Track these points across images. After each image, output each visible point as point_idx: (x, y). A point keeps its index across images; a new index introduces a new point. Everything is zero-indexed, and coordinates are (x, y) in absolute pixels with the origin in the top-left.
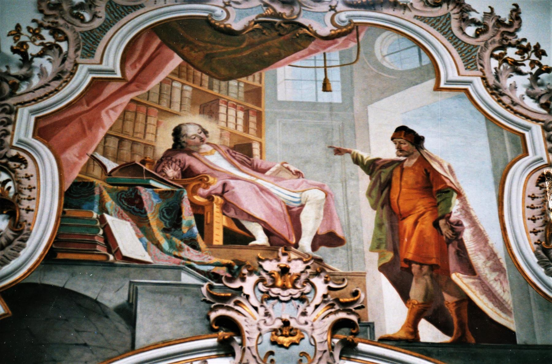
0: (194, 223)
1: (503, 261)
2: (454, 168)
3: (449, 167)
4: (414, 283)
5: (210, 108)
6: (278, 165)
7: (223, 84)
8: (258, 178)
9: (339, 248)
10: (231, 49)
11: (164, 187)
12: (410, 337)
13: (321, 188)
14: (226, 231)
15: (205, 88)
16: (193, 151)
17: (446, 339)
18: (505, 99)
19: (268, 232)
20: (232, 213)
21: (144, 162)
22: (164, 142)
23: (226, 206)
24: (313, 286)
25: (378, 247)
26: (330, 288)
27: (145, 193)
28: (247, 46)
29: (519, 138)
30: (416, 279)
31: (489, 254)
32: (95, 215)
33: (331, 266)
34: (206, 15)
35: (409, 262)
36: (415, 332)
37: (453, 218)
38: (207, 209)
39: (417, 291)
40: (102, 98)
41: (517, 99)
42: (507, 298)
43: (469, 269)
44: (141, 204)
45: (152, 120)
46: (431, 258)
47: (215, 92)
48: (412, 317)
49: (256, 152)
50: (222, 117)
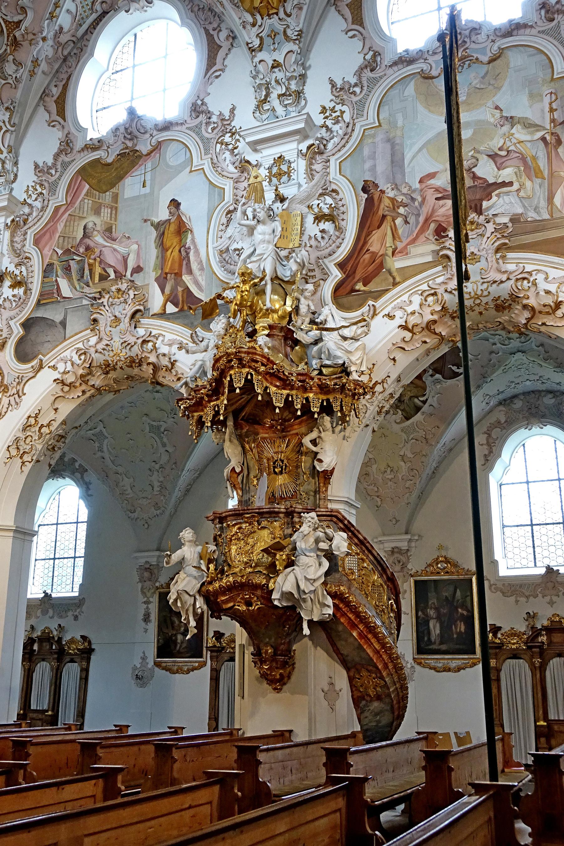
1: (204, 264)
5: (97, 212)
11: (78, 258)
17: (177, 310)
18: (219, 169)
19: (115, 272)
20: (103, 266)
21: (72, 248)
22: (80, 234)
23: (100, 263)
27: (72, 263)
32: (54, 279)
35: (166, 274)
36: (165, 310)
40: (58, 217)
41: (224, 166)
42: (203, 283)
43: (190, 272)
44: (70, 270)
45: (76, 224)
49: (114, 230)
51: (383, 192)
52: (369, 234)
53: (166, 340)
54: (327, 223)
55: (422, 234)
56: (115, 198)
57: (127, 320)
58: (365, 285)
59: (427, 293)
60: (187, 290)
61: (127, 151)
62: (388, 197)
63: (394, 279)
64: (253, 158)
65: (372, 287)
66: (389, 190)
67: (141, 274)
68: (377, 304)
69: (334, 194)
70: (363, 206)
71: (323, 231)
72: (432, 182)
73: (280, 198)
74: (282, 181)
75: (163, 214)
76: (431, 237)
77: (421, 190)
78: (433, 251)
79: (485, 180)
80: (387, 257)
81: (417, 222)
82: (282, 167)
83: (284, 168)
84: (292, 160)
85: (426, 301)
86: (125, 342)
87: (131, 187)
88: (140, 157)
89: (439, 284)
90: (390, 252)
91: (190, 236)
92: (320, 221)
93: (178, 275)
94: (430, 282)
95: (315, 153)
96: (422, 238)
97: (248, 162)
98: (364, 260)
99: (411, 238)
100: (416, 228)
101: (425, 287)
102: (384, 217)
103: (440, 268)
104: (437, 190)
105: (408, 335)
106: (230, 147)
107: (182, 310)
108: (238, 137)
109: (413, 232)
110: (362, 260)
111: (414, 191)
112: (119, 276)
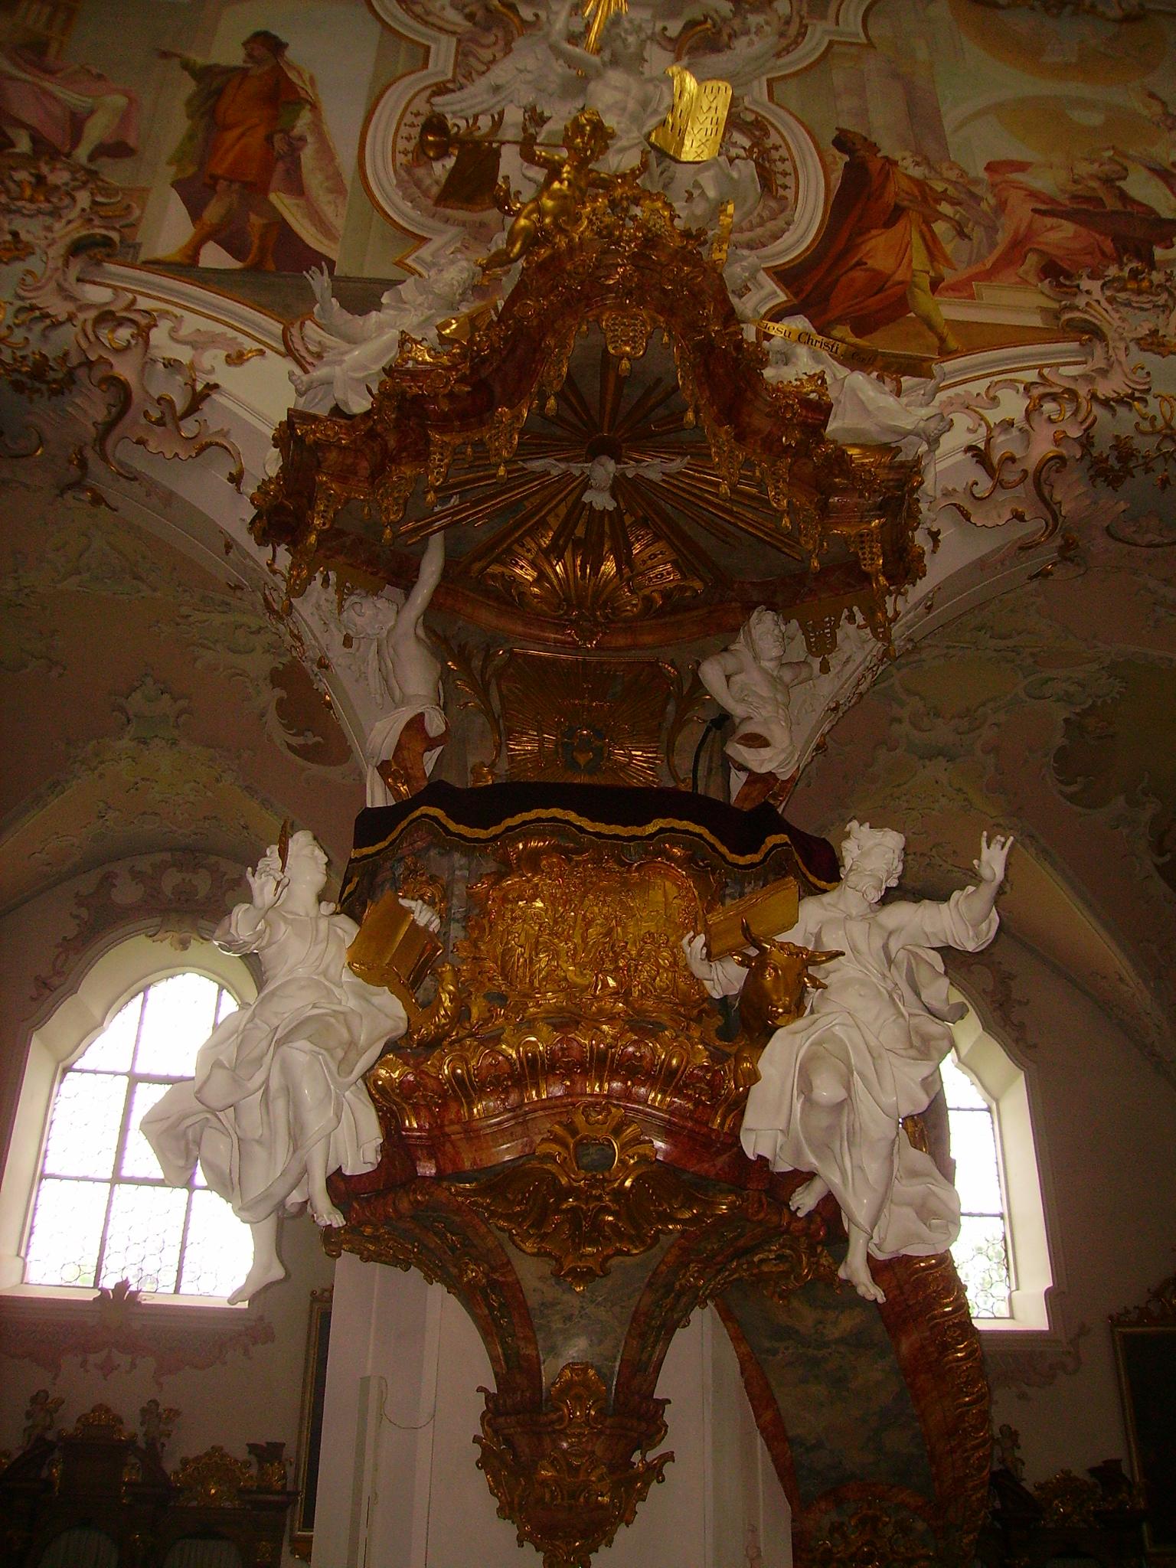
13: (126, 93)
35: (215, 179)
37: (296, 132)
39: (213, 213)
52: (862, 230)
53: (185, 331)
59: (1041, 390)
63: (942, 340)
66: (908, 162)
77: (994, 185)
78: (1043, 310)
79: (1152, 211)
81: (992, 246)
86: (33, 308)
90: (925, 281)
93: (256, 189)
100: (990, 253)
101: (1032, 376)
104: (1033, 194)
105: (985, 484)
111: (976, 182)
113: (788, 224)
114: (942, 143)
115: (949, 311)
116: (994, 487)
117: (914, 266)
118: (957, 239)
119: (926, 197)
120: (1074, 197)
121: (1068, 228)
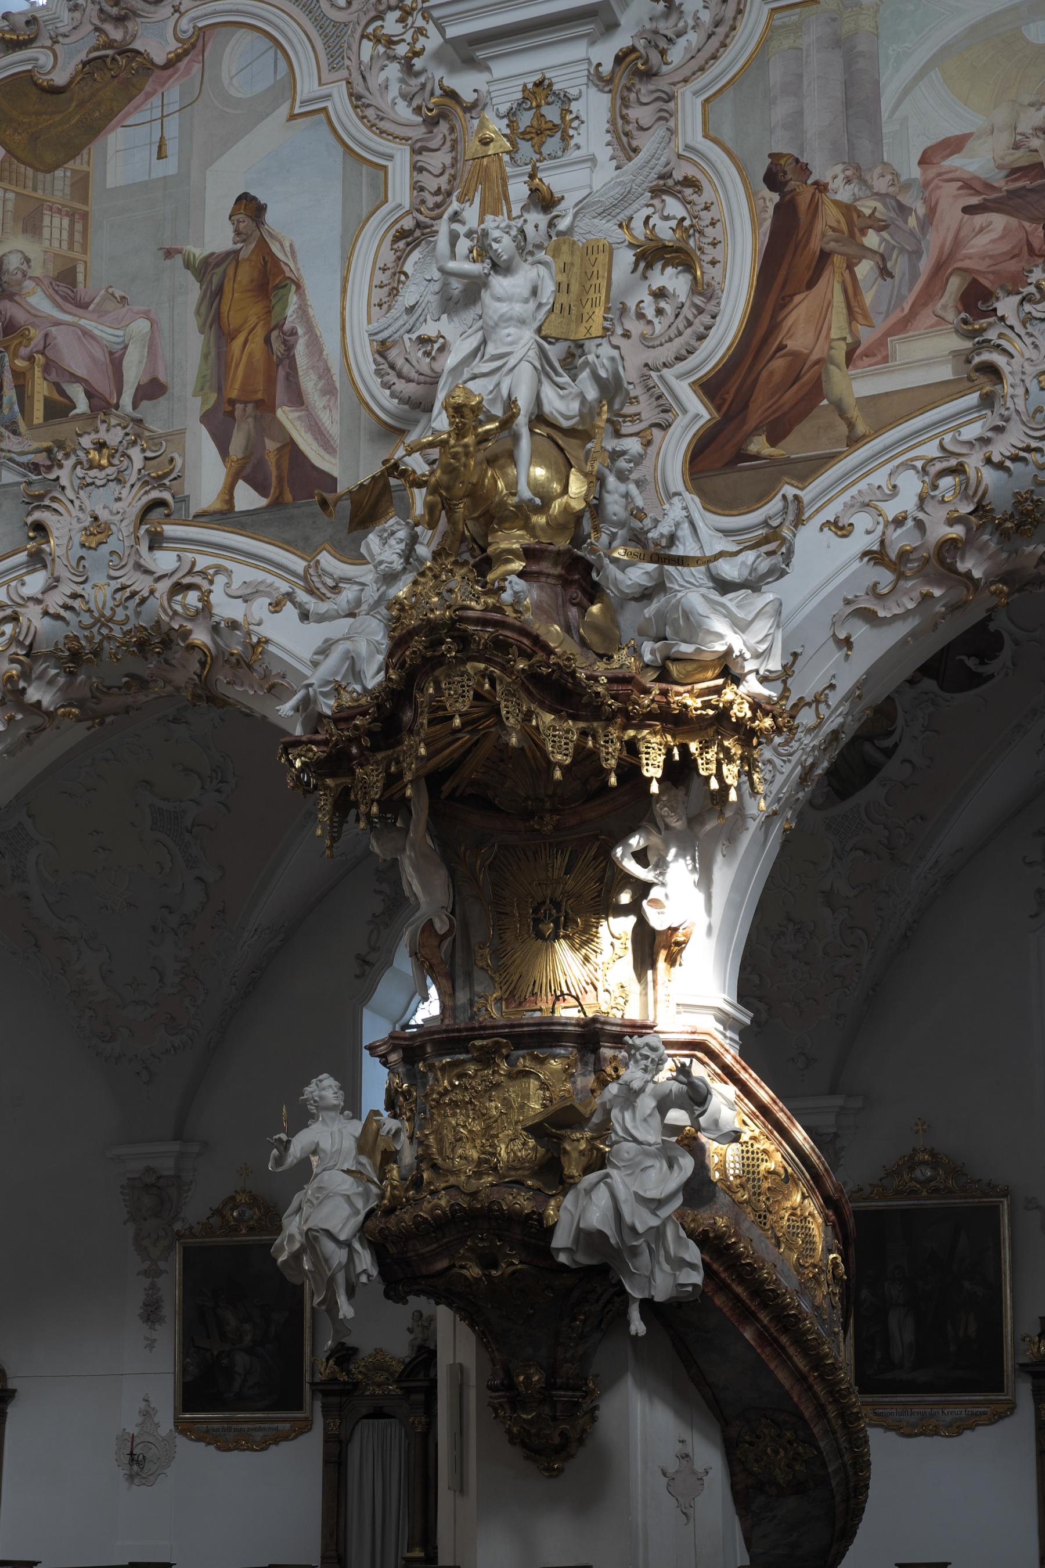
0: (15, 399)
1: (336, 378)
2: (296, 247)
3: (291, 246)
4: (235, 431)
6: (103, 292)
7: (49, 177)
8: (81, 318)
9: (161, 399)
10: (58, 117)
12: (225, 507)
13: (147, 315)
14: (48, 402)
15: (28, 192)
16: (14, 294)
17: (263, 502)
18: (370, 113)
19: (89, 395)
20: (53, 377)
23: (47, 368)
24: (129, 457)
25: (202, 389)
26: (146, 459)
28: (77, 106)
29: (382, 173)
30: (239, 426)
31: (321, 371)
33: (151, 427)
34: (30, 67)
35: (232, 402)
36: (230, 501)
37: (287, 327)
38: (28, 376)
39: (237, 445)
43: (297, 399)
46: (256, 392)
47: (39, 194)
48: (230, 479)
49: (80, 277)
50: (46, 232)
51: (821, 187)
52: (784, 302)
53: (236, 584)
54: (670, 270)
55: (925, 304)
56: (81, 185)
57: (126, 528)
58: (773, 442)
59: (939, 466)
60: (291, 448)
61: (109, 52)
62: (837, 203)
63: (851, 425)
64: (466, 84)
65: (795, 446)
66: (839, 182)
67: (162, 400)
68: (806, 495)
69: (688, 191)
70: (768, 224)
71: (660, 294)
72: (955, 161)
73: (544, 199)
74: (546, 150)
75: (218, 236)
76: (950, 316)
77: (926, 185)
78: (956, 354)
80: (832, 367)
82: (545, 110)
83: (552, 113)
84: (573, 92)
85: (935, 487)
86: (123, 588)
87: (124, 155)
88: (148, 67)
89: (970, 444)
90: (840, 353)
91: (293, 299)
92: (649, 266)
93: (265, 406)
94: (948, 438)
95: (635, 72)
96: (926, 318)
97: (452, 95)
98: (771, 374)
99: (897, 315)
100: (910, 290)
101: (931, 450)
102: (825, 257)
103: (973, 399)
104: (968, 185)
106: (402, 50)
107: (277, 503)
108: (420, 22)
109: (901, 298)
110: (764, 374)
111: (907, 186)
112: (101, 406)
113: (714, 317)
114: (877, 140)
115: (860, 385)
116: (898, 580)
117: (833, 336)
118: (880, 281)
119: (855, 222)
120: (1015, 172)
121: (998, 221)
